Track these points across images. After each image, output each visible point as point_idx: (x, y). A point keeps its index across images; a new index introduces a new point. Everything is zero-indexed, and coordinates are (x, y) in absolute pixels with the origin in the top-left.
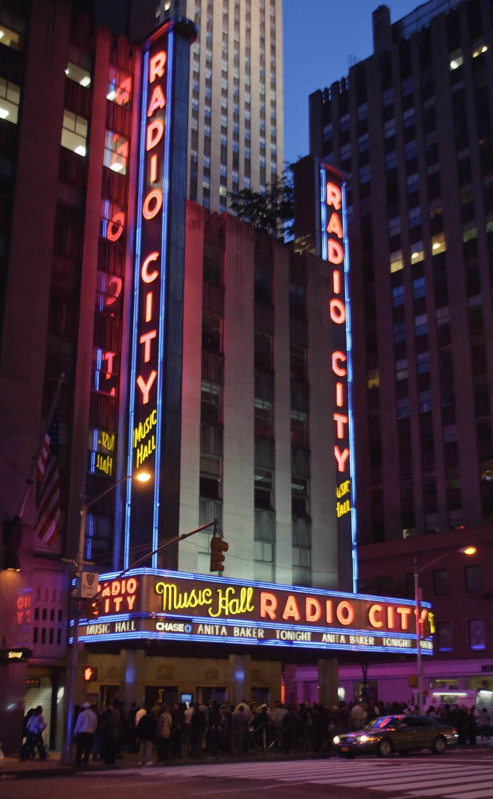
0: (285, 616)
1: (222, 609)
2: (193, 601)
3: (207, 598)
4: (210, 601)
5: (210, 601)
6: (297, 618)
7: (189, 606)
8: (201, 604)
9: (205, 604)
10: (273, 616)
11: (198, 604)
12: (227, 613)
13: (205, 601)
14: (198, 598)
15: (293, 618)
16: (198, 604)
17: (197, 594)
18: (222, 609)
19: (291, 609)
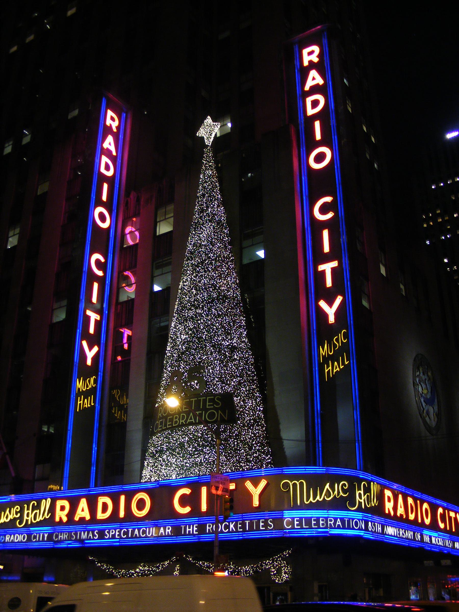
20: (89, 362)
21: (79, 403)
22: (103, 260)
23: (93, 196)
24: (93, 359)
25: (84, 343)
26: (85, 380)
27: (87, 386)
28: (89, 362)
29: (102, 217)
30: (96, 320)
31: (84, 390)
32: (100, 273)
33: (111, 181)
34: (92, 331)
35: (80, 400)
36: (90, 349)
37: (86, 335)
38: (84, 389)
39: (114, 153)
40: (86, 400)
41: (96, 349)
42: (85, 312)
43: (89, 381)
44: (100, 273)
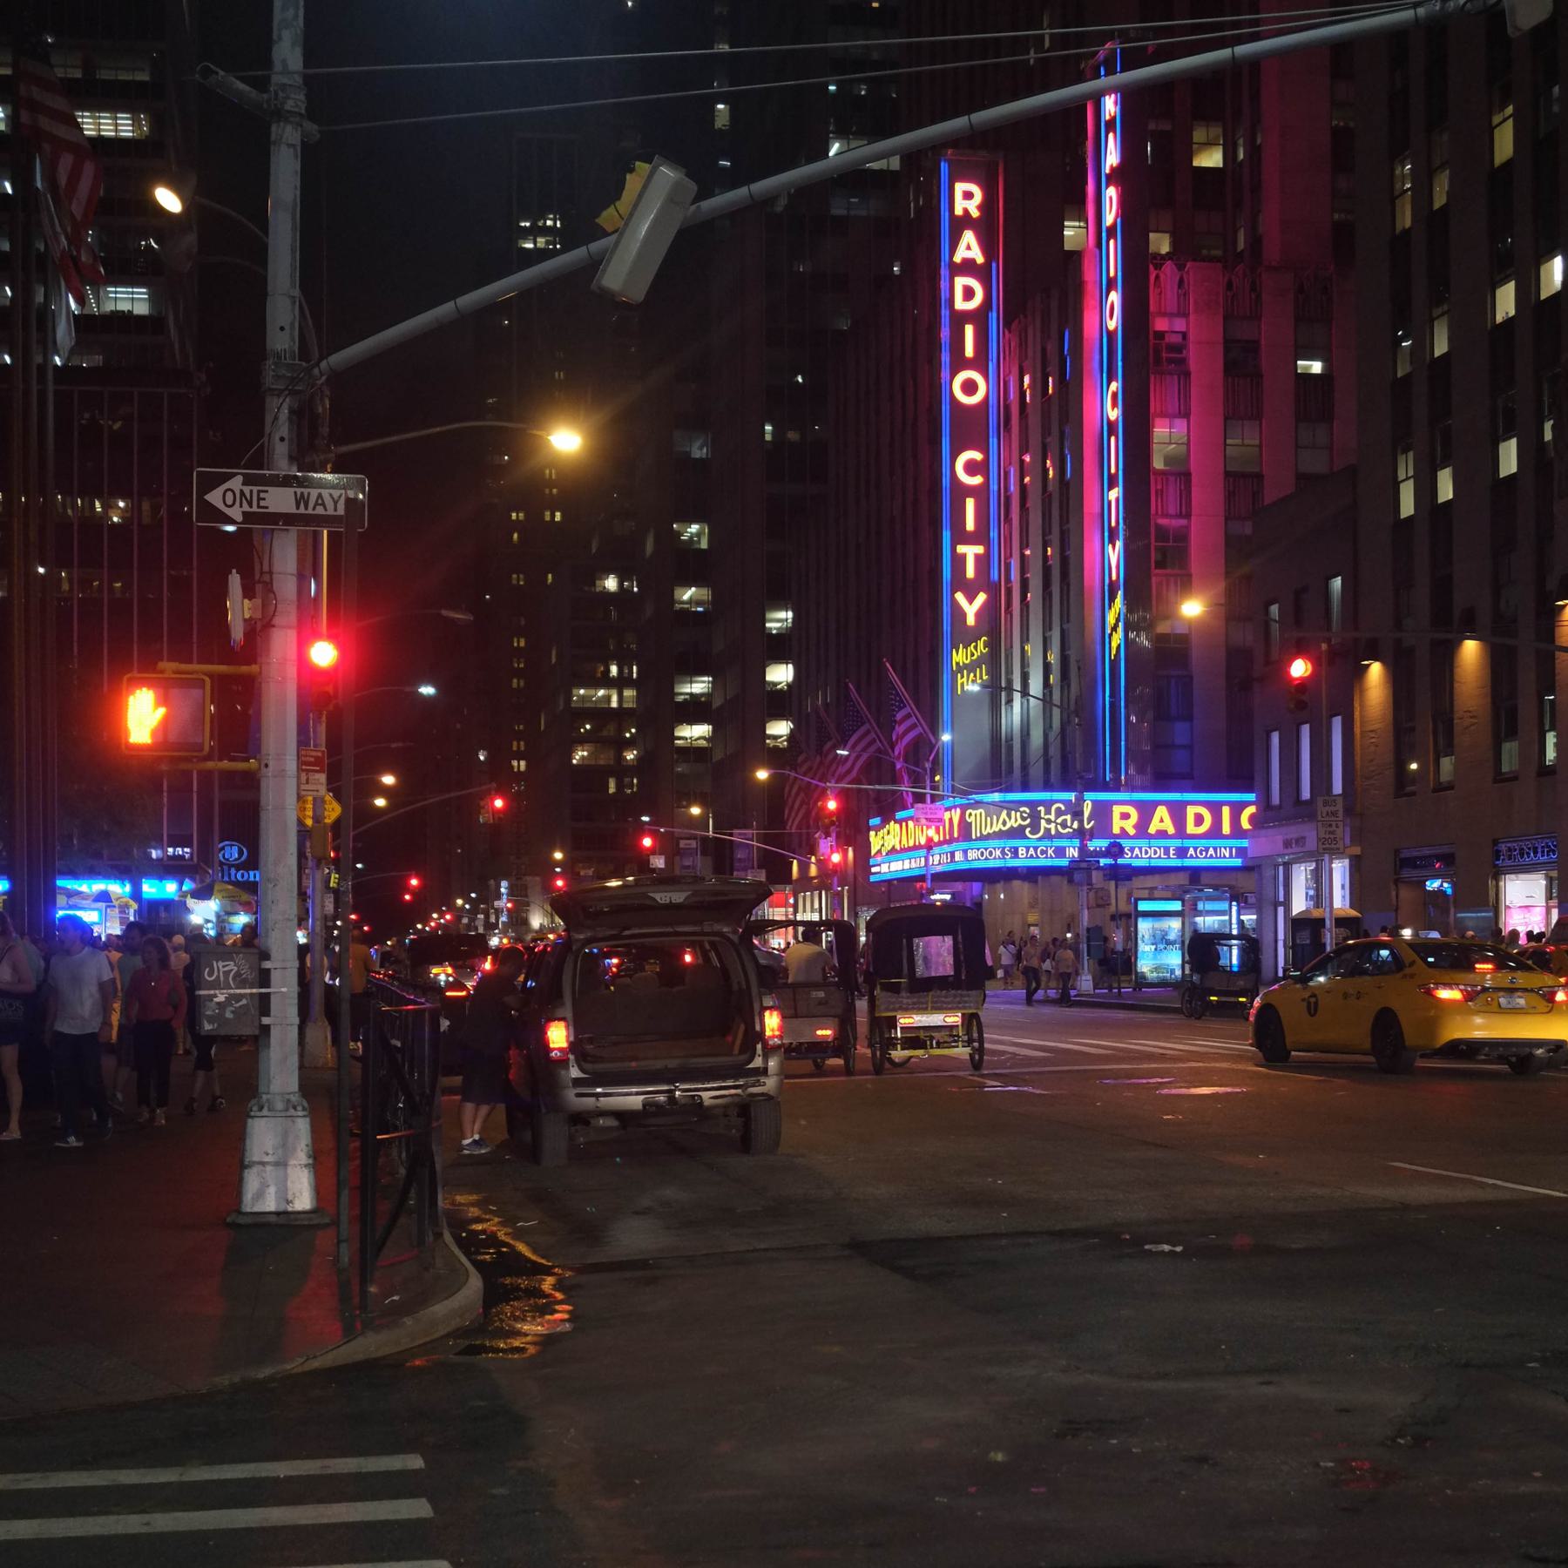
0: (1152, 830)
1: (1045, 828)
2: (1004, 823)
3: (1024, 819)
4: (1028, 821)
5: (1028, 821)
6: (1171, 830)
7: (1000, 829)
8: (1015, 825)
9: (1020, 825)
10: (1132, 832)
11: (1012, 827)
12: (1053, 832)
13: (1020, 821)
14: (1010, 818)
15: (1166, 832)
16: (1012, 827)
17: (1009, 816)
18: (1045, 828)
19: (1162, 821)
20: (971, 621)
21: (959, 682)
22: (977, 456)
23: (945, 358)
24: (978, 615)
25: (960, 597)
26: (966, 647)
27: (973, 655)
28: (971, 621)
29: (970, 387)
30: (977, 557)
31: (967, 662)
32: (977, 480)
33: (979, 317)
34: (970, 572)
35: (962, 677)
36: (971, 600)
37: (960, 582)
38: (967, 659)
39: (980, 260)
40: (972, 675)
41: (981, 598)
42: (953, 550)
43: (976, 648)
44: (977, 480)
